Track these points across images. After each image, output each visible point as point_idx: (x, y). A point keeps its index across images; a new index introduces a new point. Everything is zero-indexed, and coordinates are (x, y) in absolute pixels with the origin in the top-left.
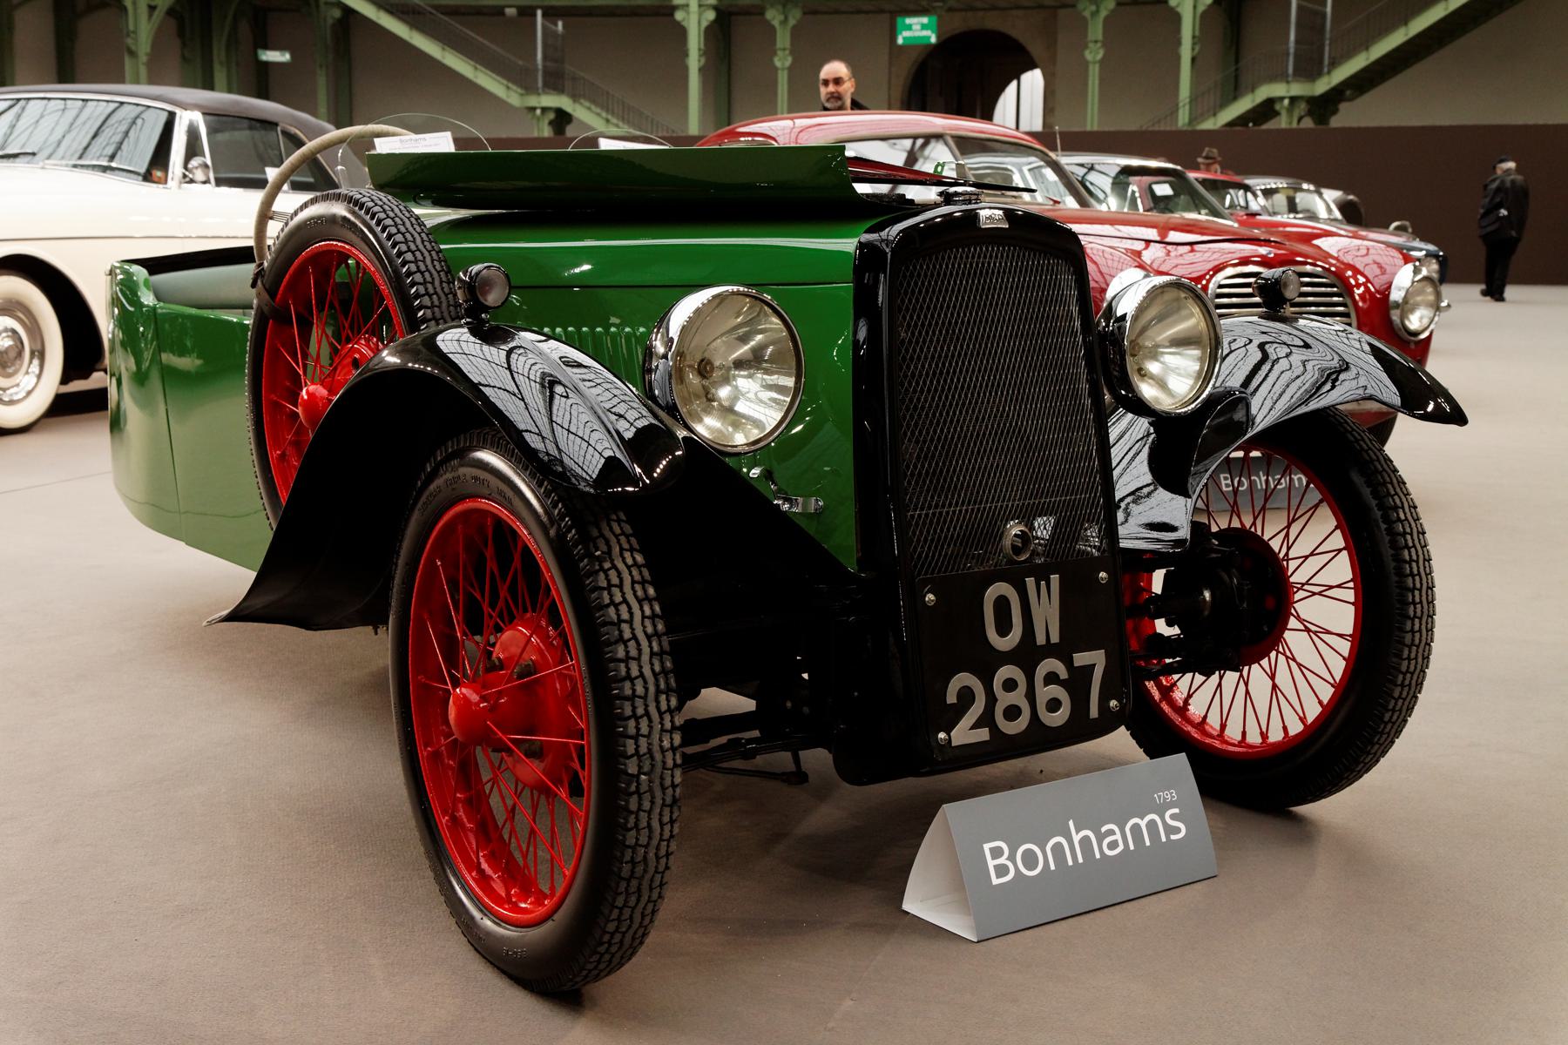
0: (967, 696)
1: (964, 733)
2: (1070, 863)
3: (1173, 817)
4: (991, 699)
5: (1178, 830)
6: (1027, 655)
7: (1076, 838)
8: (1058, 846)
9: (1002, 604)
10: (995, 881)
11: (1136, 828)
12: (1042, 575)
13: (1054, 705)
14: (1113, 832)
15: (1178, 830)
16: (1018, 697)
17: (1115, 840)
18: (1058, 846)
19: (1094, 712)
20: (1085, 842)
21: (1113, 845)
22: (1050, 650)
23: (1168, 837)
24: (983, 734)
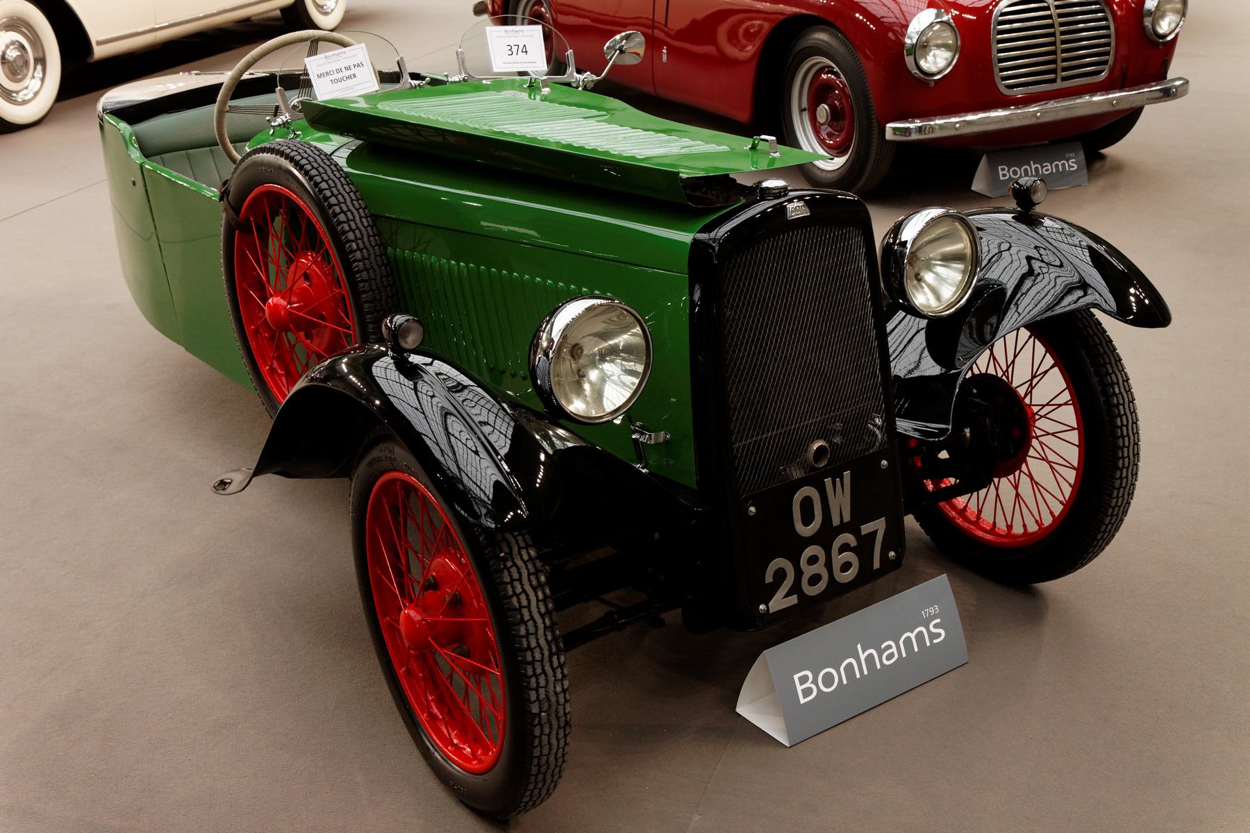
0: (780, 575)
1: (779, 602)
2: (858, 676)
3: (936, 626)
4: (799, 573)
5: (940, 635)
6: (825, 537)
7: (863, 657)
8: (849, 668)
9: (807, 503)
10: (803, 701)
11: (908, 640)
12: (836, 474)
13: (846, 566)
14: (889, 647)
15: (939, 635)
16: (819, 568)
17: (892, 652)
18: (850, 664)
19: (877, 564)
20: (870, 659)
21: (890, 657)
22: (844, 528)
23: (931, 641)
24: (793, 600)
